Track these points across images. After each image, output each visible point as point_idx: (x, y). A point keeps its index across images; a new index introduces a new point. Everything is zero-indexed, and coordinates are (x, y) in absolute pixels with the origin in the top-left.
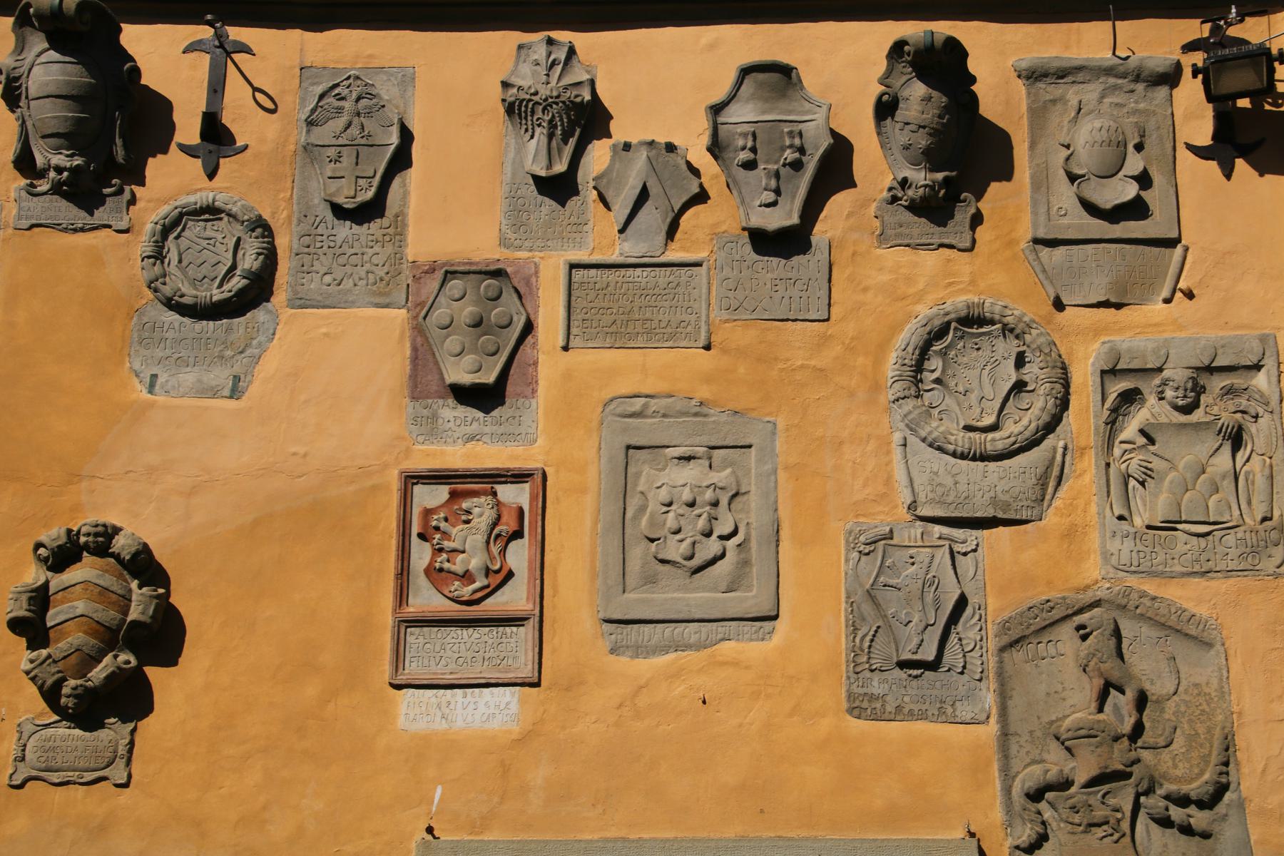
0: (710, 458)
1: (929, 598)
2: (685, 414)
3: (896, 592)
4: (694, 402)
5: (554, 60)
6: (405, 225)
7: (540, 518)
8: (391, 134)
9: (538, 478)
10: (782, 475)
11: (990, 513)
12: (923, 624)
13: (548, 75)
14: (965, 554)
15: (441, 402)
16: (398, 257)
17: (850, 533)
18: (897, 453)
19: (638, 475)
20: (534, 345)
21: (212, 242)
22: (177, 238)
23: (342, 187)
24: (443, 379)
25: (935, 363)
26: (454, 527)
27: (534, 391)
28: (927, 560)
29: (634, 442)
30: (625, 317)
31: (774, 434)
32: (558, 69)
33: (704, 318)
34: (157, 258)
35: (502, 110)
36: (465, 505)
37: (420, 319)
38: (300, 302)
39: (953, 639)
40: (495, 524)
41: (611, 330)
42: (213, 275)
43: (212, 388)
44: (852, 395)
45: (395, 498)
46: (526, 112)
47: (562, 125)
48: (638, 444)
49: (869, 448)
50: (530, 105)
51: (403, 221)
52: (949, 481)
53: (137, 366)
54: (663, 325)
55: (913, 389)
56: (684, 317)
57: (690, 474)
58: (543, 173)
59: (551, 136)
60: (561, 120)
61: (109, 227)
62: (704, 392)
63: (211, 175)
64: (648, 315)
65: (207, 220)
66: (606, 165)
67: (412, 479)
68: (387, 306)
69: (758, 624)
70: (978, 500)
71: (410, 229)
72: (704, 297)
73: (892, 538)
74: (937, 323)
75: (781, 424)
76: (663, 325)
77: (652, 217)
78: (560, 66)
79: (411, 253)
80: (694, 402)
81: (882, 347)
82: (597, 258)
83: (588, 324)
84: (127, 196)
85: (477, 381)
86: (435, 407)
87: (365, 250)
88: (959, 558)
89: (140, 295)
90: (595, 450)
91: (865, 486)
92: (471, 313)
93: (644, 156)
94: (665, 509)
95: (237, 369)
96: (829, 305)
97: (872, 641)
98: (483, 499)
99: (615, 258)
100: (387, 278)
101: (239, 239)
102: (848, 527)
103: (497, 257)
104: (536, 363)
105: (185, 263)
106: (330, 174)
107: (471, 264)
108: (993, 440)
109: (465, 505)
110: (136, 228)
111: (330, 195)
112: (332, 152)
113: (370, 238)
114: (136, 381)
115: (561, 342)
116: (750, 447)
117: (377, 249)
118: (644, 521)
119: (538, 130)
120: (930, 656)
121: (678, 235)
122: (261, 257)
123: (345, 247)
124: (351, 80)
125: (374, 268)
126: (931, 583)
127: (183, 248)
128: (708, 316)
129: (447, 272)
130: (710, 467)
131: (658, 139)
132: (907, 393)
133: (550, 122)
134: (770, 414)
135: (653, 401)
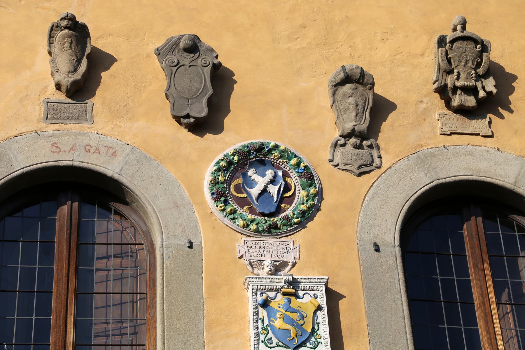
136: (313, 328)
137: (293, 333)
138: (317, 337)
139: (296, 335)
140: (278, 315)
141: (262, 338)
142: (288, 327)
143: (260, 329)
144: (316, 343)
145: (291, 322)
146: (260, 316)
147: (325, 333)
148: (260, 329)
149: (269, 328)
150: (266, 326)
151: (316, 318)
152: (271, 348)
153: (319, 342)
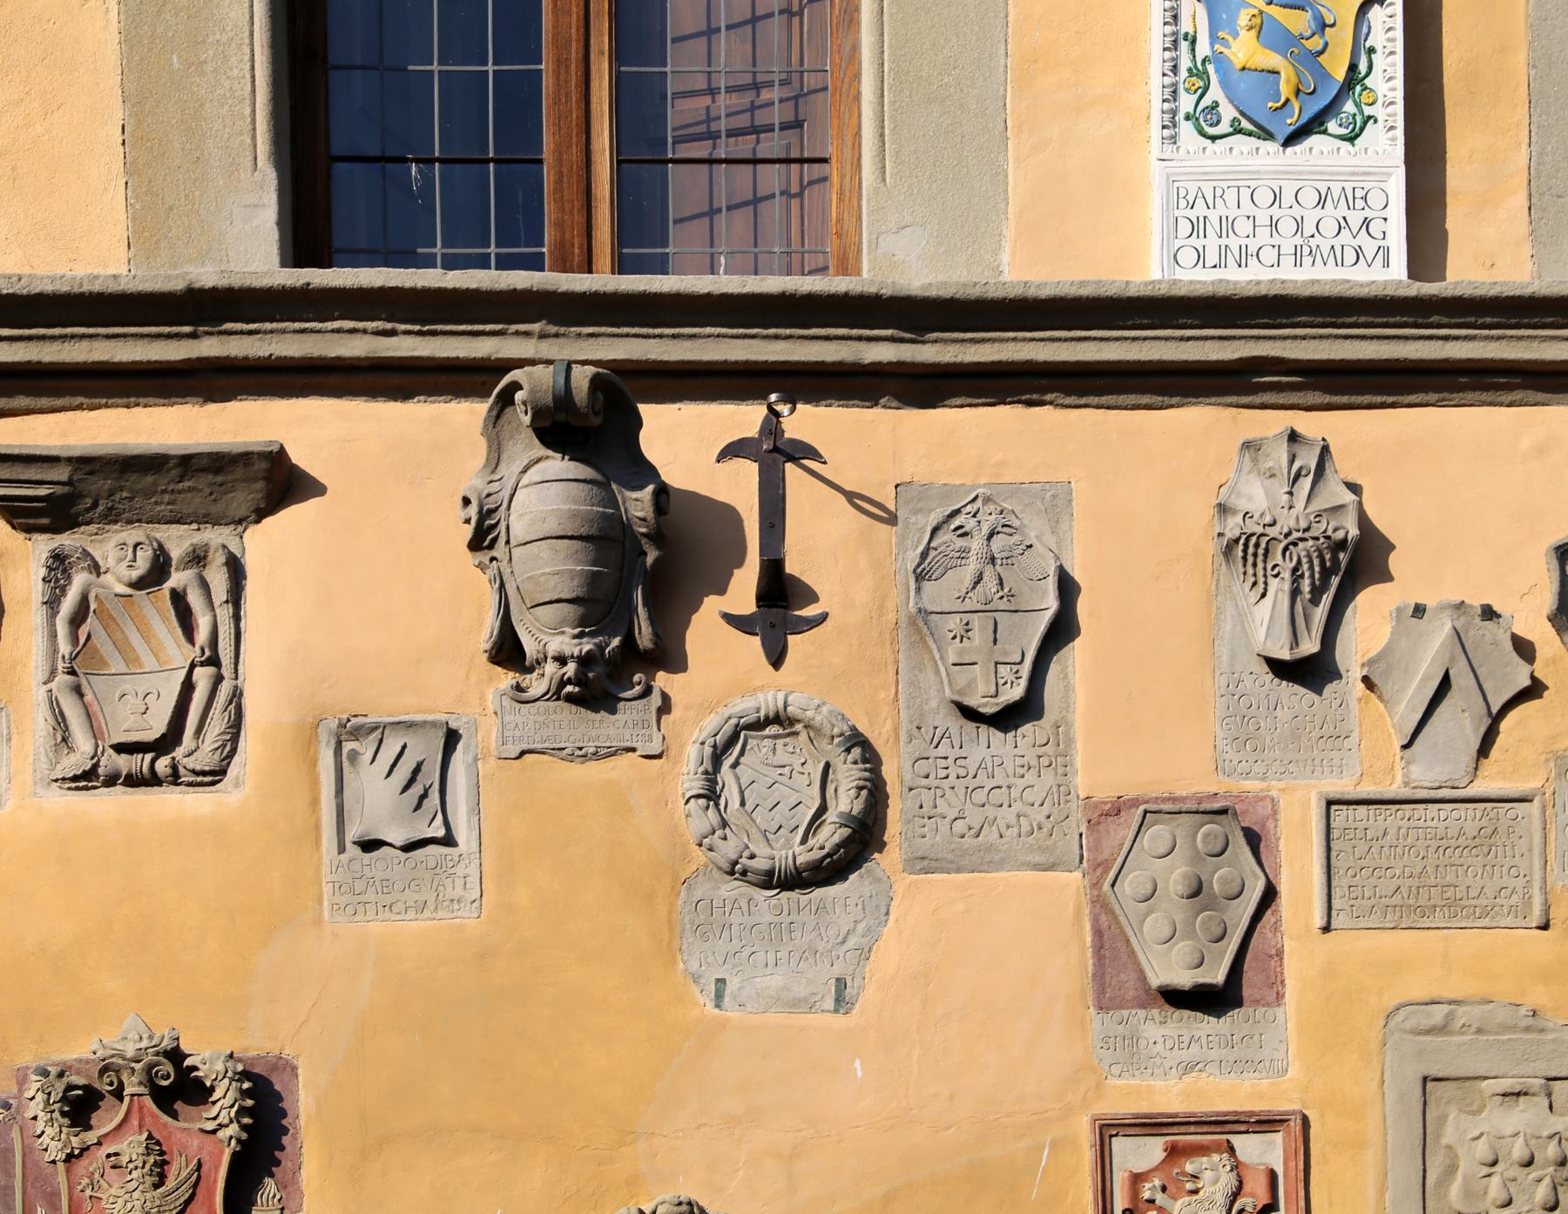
0: (1549, 1095)
2: (1512, 1028)
4: (1523, 1011)
5: (1301, 468)
6: (1070, 741)
7: (1302, 1185)
8: (1045, 592)
9: (1295, 1125)
13: (1291, 493)
15: (1142, 1013)
16: (1063, 791)
19: (1442, 1120)
20: (1276, 927)
21: (786, 770)
22: (735, 765)
23: (974, 680)
24: (1143, 978)
26: (1175, 1198)
27: (1280, 997)
29: (1435, 1071)
30: (1415, 882)
32: (1306, 483)
33: (1537, 883)
34: (708, 798)
35: (1212, 548)
36: (1189, 1167)
37: (1106, 886)
38: (923, 864)
40: (1236, 1195)
41: (1392, 901)
42: (793, 824)
43: (806, 1000)
45: (1088, 1156)
46: (1255, 555)
47: (1312, 576)
48: (1440, 1075)
50: (1264, 541)
51: (1067, 734)
53: (694, 966)
54: (1473, 893)
56: (1511, 883)
57: (1519, 1123)
58: (1285, 655)
59: (1295, 593)
60: (1311, 568)
61: (633, 750)
62: (1537, 996)
63: (777, 658)
64: (1450, 878)
65: (775, 737)
66: (1385, 642)
67: (1107, 1130)
68: (1051, 867)
71: (1079, 746)
72: (1537, 850)
76: (1473, 893)
77: (1458, 723)
78: (1311, 477)
79: (1082, 784)
80: (1523, 1011)
82: (1368, 790)
83: (1357, 892)
84: (655, 700)
85: (1201, 980)
86: (1133, 1021)
87: (1012, 780)
89: (685, 856)
90: (1376, 1083)
92: (1185, 876)
93: (1448, 626)
94: (1486, 1170)
95: (837, 970)
98: (1216, 1157)
99: (1395, 789)
100: (1047, 826)
101: (827, 766)
103: (1213, 789)
104: (1280, 954)
105: (749, 806)
106: (952, 658)
107: (1174, 800)
109: (1189, 1167)
110: (673, 752)
111: (959, 692)
112: (954, 623)
113: (1019, 761)
114: (695, 989)
115: (1319, 921)
117: (1030, 777)
118: (1455, 1190)
119: (1274, 584)
121: (1495, 752)
122: (864, 793)
123: (982, 774)
124: (979, 503)
125: (1028, 809)
127: (744, 782)
128: (1544, 879)
129: (1146, 812)
130: (1551, 1107)
131: (1467, 601)
133: (1295, 570)
135: (1461, 1010)
136: (1353, 68)
137: (1288, 81)
138: (1365, 98)
139: (1298, 92)
140: (1243, 19)
141: (1186, 103)
142: (1274, 60)
143: (1183, 73)
144: (1359, 118)
145: (1285, 42)
146: (1186, 26)
147: (1390, 84)
148: (1183, 73)
149: (1211, 68)
150: (1204, 61)
151: (1365, 30)
152: (1213, 138)
153: (1370, 117)
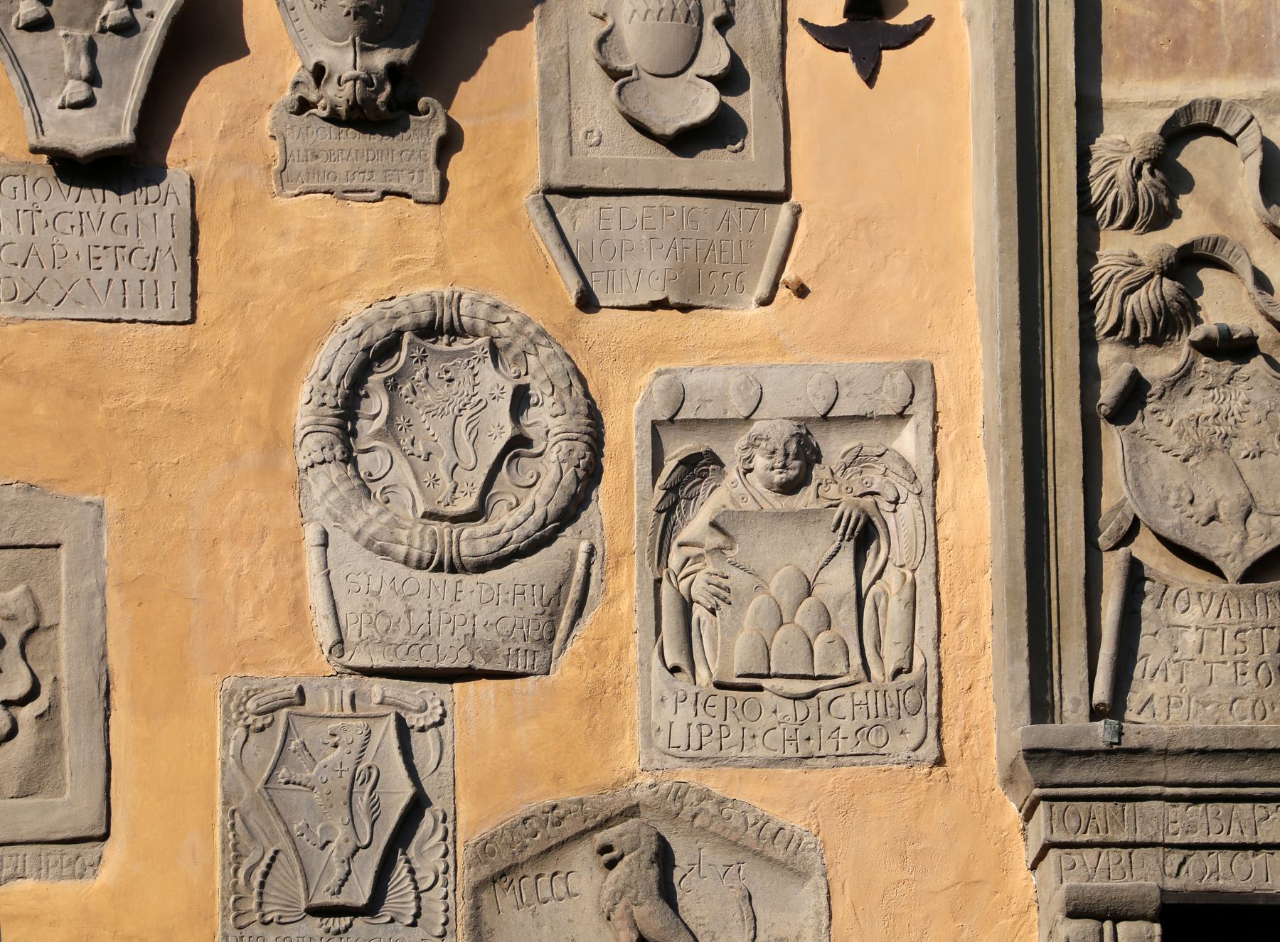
1: (361, 803)
3: (305, 795)
10: (114, 598)
11: (463, 661)
12: (350, 846)
14: (422, 730)
17: (231, 696)
18: (312, 559)
25: (377, 402)
28: (359, 740)
31: (98, 524)
39: (401, 868)
44: (234, 457)
49: (264, 551)
52: (397, 608)
55: (338, 450)
69: (72, 849)
70: (444, 639)
73: (302, 703)
74: (380, 331)
75: (112, 506)
81: (289, 371)
88: (415, 736)
91: (256, 614)
96: (194, 295)
97: (265, 875)
102: (227, 684)
108: (472, 538)
116: (58, 546)
120: (360, 893)
126: (364, 777)
132: (327, 454)
134: (92, 490)
